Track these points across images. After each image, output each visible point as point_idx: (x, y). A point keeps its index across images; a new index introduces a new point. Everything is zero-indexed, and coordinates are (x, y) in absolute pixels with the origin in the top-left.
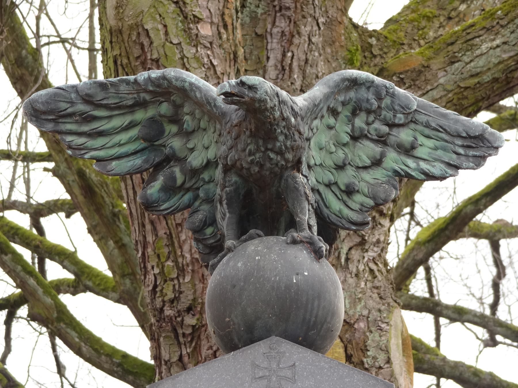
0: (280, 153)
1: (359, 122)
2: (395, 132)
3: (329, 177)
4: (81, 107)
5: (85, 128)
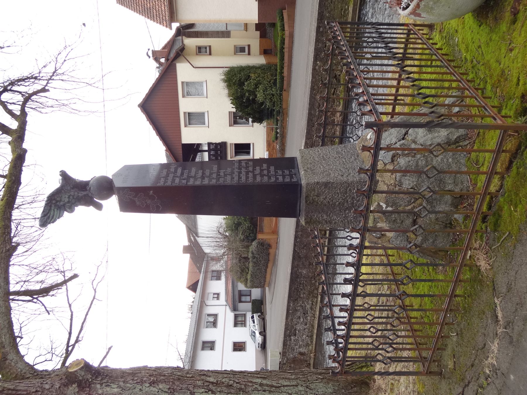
5: (50, 218)
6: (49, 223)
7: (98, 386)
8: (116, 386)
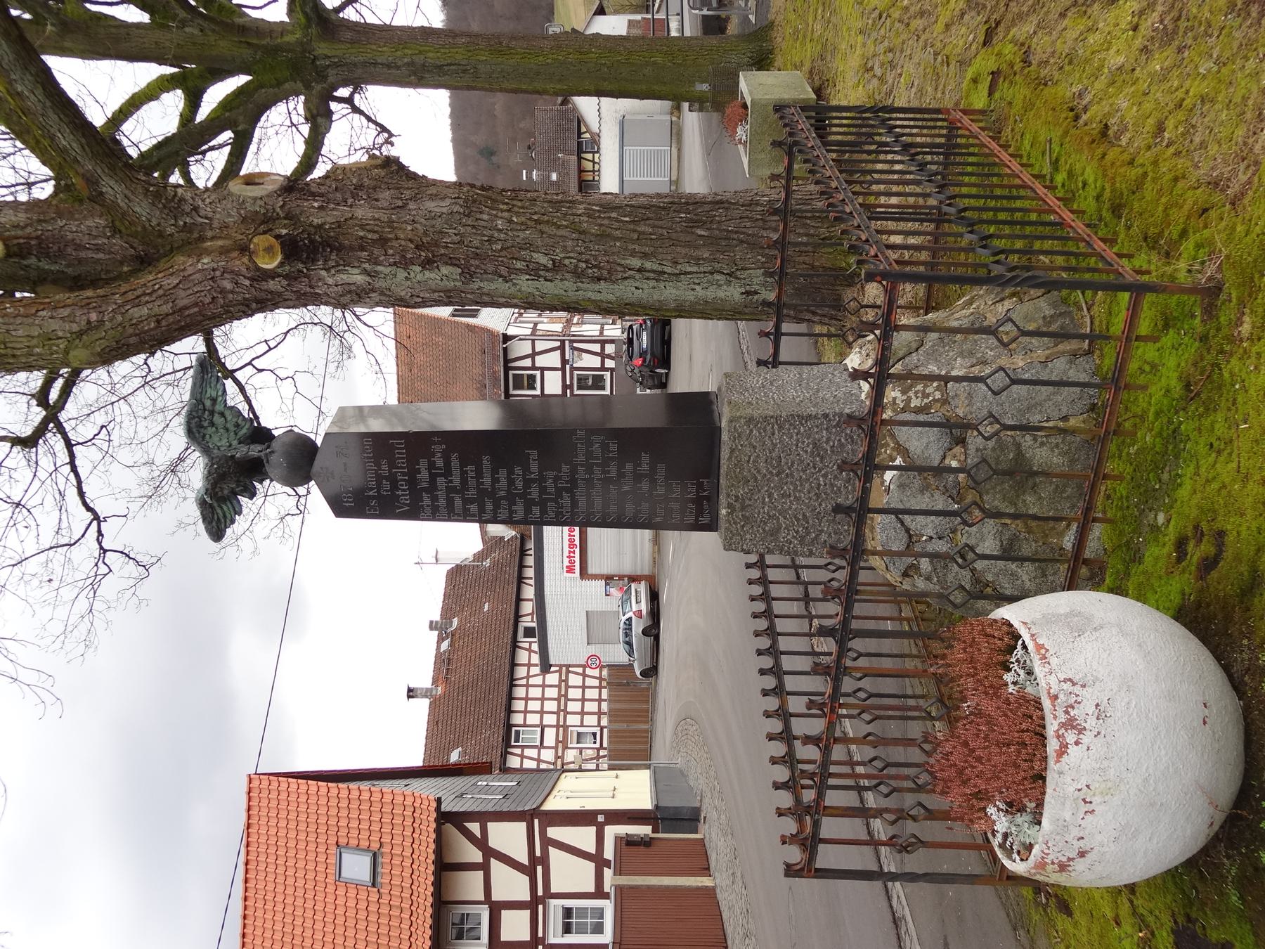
1: (206, 424)
4: (214, 524)
7: (323, 273)
8: (357, 271)
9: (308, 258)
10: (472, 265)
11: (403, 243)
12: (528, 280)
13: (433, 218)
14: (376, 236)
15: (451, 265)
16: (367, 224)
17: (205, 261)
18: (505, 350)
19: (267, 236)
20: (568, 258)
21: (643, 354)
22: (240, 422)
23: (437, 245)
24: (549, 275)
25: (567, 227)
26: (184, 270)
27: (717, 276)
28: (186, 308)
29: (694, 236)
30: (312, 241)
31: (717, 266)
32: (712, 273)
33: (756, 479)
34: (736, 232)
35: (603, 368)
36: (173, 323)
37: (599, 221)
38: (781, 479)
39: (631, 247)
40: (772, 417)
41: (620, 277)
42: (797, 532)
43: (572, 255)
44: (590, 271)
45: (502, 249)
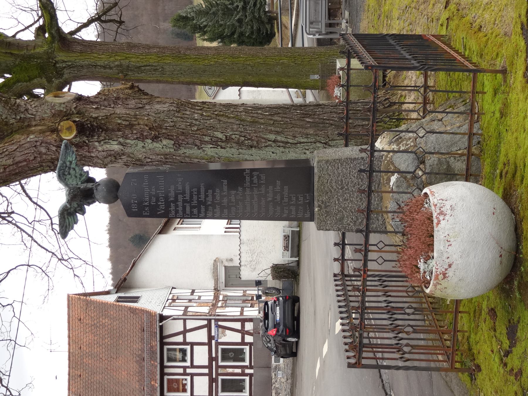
0: (78, 192)
1: (66, 173)
2: (67, 166)
3: (78, 179)
4: (64, 228)
5: (68, 227)
6: (69, 231)
7: (97, 144)
8: (115, 143)
9: (89, 134)
10: (180, 139)
11: (142, 126)
12: (211, 148)
13: (159, 113)
14: (127, 123)
15: (168, 139)
16: (123, 117)
17: (32, 137)
18: (161, 328)
19: (69, 121)
20: (234, 134)
21: (276, 325)
22: (82, 173)
23: (161, 128)
24: (223, 144)
25: (233, 118)
26: (19, 142)
27: (318, 145)
28: (20, 162)
29: (305, 122)
30: (92, 125)
31: (318, 138)
32: (315, 143)
33: (331, 191)
34: (328, 120)
35: (243, 343)
36: (12, 170)
37: (251, 115)
38: (343, 191)
39: (269, 128)
40: (337, 160)
41: (263, 145)
42: (352, 219)
43: (236, 133)
44: (247, 142)
45: (198, 130)
